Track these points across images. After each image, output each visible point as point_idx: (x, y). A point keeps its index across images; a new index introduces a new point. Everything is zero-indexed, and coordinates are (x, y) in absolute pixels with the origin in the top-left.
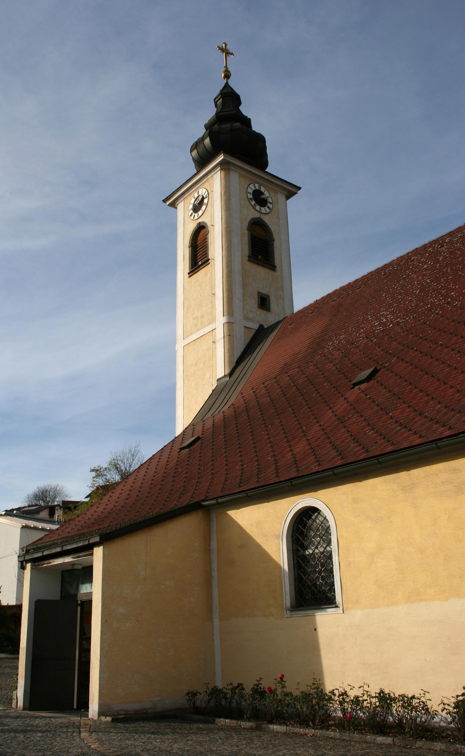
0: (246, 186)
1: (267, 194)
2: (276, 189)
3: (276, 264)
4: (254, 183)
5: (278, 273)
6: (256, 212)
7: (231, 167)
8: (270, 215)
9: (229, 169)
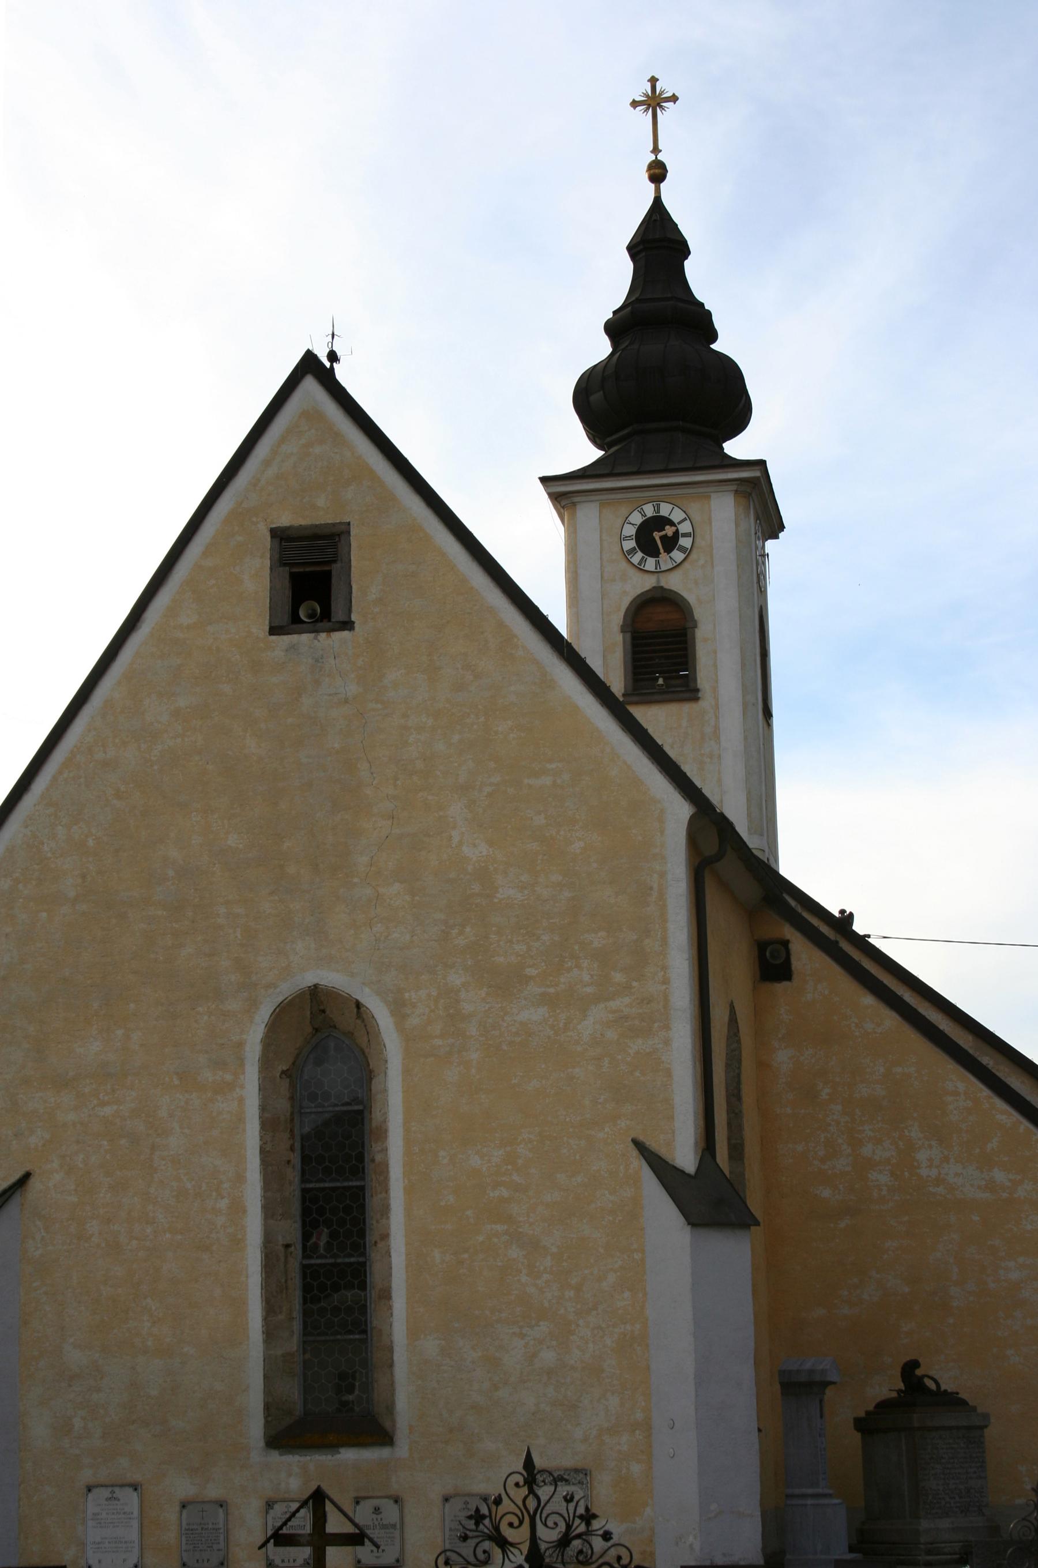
0: (620, 521)
1: (677, 516)
2: (701, 490)
3: (699, 686)
4: (639, 508)
5: (705, 703)
6: (646, 576)
7: (576, 499)
8: (686, 565)
9: (574, 504)
